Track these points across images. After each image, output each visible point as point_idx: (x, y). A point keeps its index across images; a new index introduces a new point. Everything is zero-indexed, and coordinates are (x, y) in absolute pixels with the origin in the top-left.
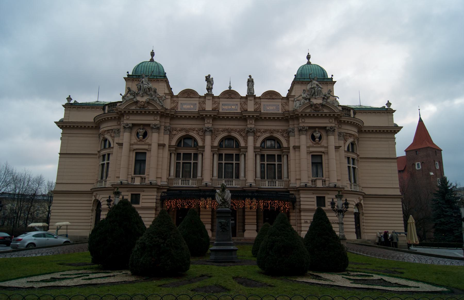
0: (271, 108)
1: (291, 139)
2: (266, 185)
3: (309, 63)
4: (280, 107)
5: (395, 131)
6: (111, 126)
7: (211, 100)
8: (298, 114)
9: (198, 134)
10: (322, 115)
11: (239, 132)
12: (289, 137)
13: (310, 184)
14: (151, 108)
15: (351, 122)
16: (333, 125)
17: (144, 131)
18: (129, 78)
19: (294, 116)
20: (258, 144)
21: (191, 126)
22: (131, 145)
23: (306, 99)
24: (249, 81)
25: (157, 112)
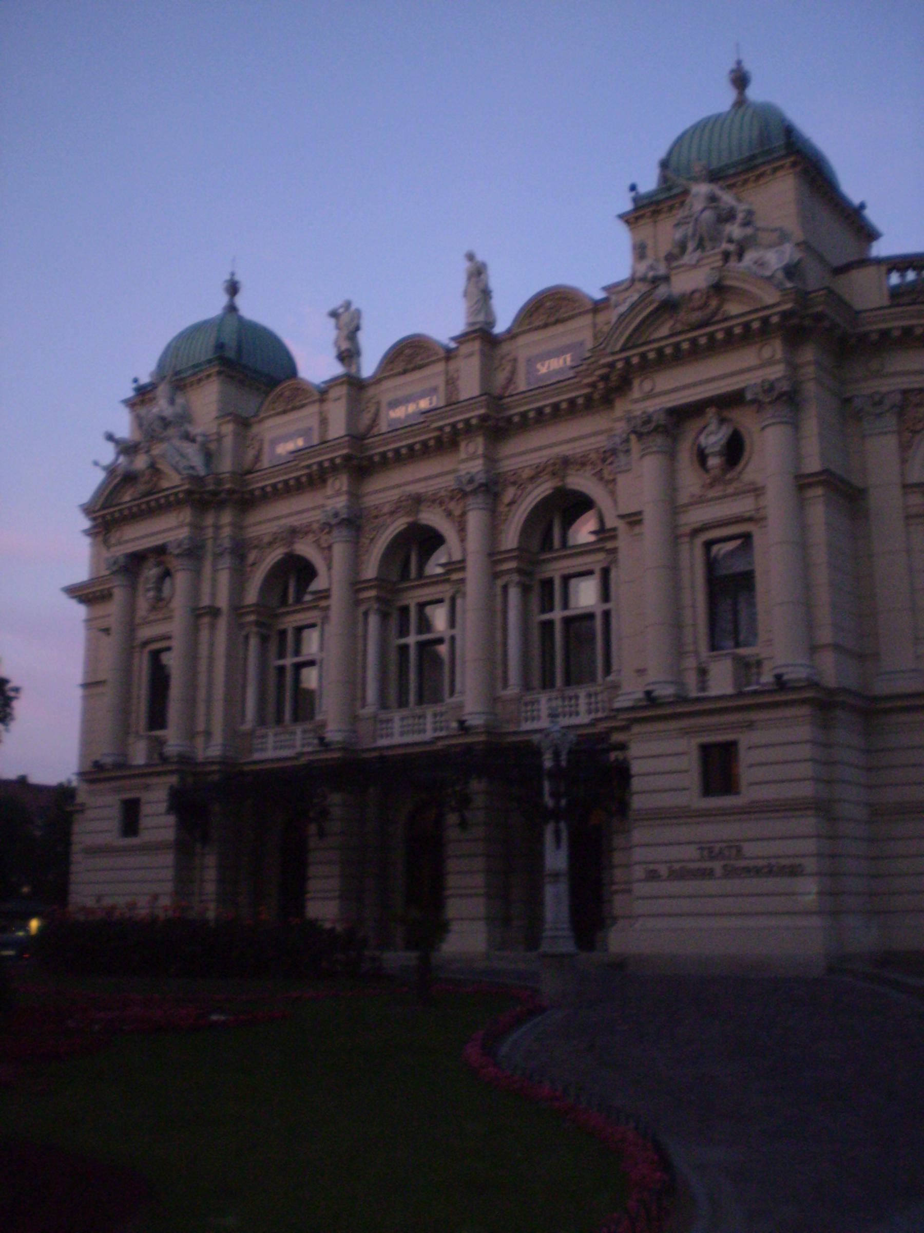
0: (555, 364)
8: (611, 365)
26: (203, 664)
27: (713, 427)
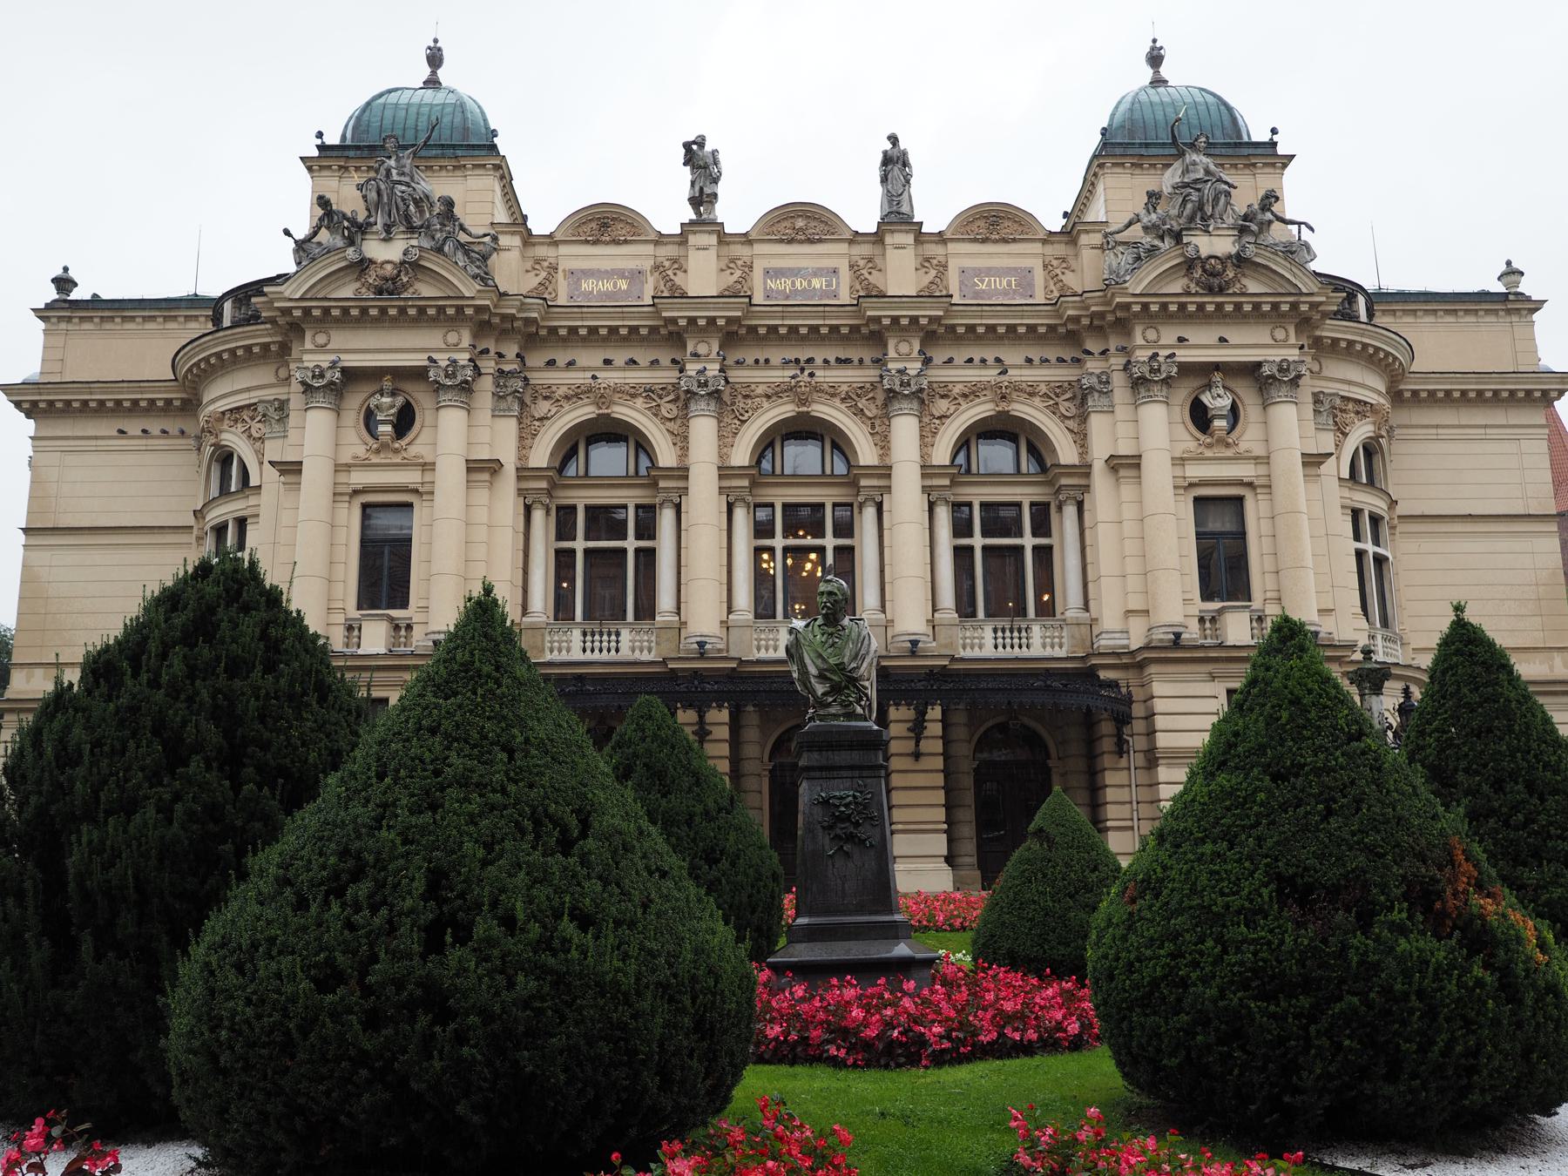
1: (1097, 423)
2: (983, 643)
3: (1158, 82)
4: (1039, 276)
5: (1545, 393)
6: (248, 390)
7: (713, 253)
8: (1127, 306)
9: (656, 412)
10: (1238, 306)
11: (848, 399)
12: (1083, 418)
13: (1192, 633)
14: (426, 290)
15: (1365, 346)
16: (1293, 354)
17: (400, 401)
18: (327, 159)
19: (1110, 318)
20: (942, 454)
21: (625, 381)
22: (339, 468)
23: (1162, 238)
24: (887, 160)
25: (460, 309)
26: (481, 534)
27: (1221, 391)
